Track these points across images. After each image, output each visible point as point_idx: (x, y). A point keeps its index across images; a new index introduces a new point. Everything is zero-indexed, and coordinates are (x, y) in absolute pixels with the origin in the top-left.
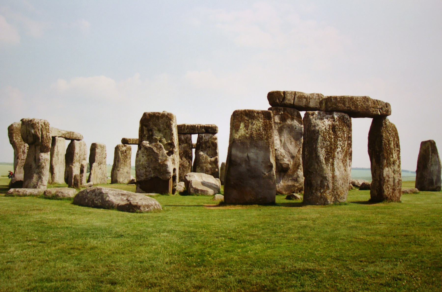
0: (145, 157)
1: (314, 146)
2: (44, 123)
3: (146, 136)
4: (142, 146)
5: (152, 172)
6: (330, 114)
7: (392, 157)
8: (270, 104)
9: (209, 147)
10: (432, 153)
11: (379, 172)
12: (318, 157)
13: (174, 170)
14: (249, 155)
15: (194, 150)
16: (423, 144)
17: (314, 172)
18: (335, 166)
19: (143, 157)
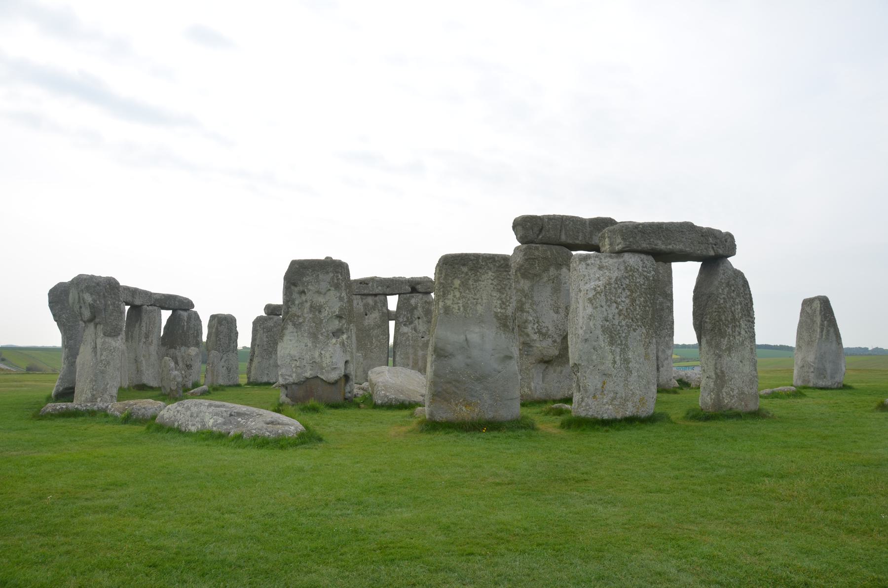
5: (308, 367)
8: (520, 239)
13: (346, 362)
14: (468, 336)
15: (392, 324)
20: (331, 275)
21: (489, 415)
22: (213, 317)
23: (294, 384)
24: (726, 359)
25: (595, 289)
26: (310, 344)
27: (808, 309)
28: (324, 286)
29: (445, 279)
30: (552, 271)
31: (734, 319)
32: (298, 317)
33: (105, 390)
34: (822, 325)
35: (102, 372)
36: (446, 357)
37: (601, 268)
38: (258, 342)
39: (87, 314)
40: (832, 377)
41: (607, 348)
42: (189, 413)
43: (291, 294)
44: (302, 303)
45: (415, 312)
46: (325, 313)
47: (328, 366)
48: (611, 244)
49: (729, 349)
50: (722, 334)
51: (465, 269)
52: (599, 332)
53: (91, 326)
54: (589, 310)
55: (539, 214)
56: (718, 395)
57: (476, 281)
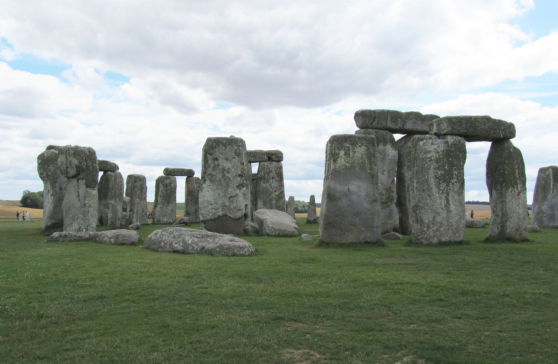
0: (210, 192)
1: (426, 177)
3: (212, 166)
4: (207, 179)
5: (220, 209)
6: (443, 139)
7: (517, 189)
9: (273, 178)
10: (554, 182)
11: (501, 206)
12: (430, 189)
13: (246, 205)
14: (350, 187)
16: (542, 171)
17: (426, 207)
18: (450, 199)
19: (208, 191)
22: (130, 177)
23: (210, 220)
27: (543, 175)
30: (381, 147)
34: (554, 185)
36: (335, 200)
39: (72, 172)
41: (437, 195)
42: (172, 235)
45: (271, 174)
47: (234, 208)
48: (438, 129)
53: (74, 181)
56: (503, 227)
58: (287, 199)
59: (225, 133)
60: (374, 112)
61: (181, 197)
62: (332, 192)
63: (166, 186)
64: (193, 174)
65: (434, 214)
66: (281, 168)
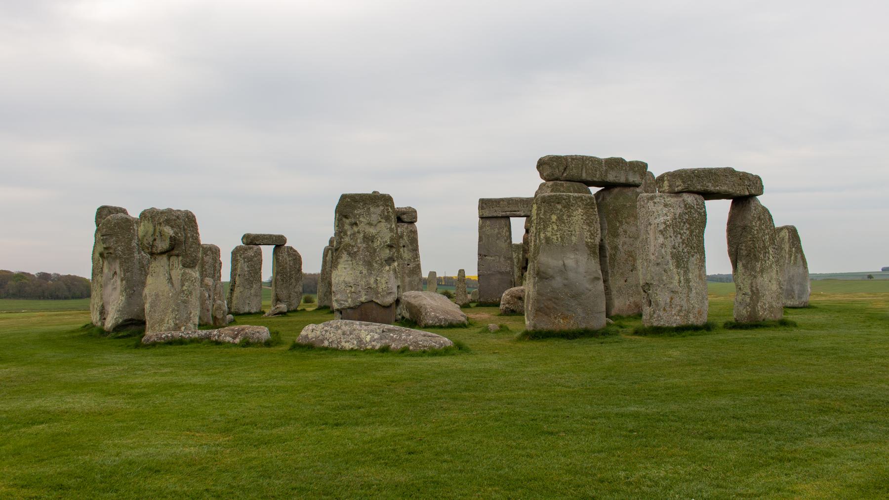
2: (187, 217)
5: (363, 293)
8: (542, 176)
13: (398, 287)
14: (566, 262)
20: (382, 208)
21: (583, 326)
23: (349, 308)
24: (759, 280)
25: (665, 223)
26: (365, 272)
28: (374, 218)
29: (544, 214)
31: (765, 247)
32: (353, 246)
33: (189, 319)
34: (790, 251)
35: (184, 302)
37: (666, 205)
38: (239, 271)
40: (800, 297)
42: (340, 331)
43: (343, 225)
44: (354, 234)
46: (376, 244)
48: (670, 186)
49: (762, 271)
50: (757, 259)
51: (559, 207)
52: (669, 257)
54: (661, 240)
55: (563, 155)
57: (569, 216)
58: (425, 274)
59: (365, 188)
60: (565, 158)
61: (267, 273)
62: (542, 269)
63: (249, 260)
64: (285, 242)
65: (672, 294)
66: (415, 232)
